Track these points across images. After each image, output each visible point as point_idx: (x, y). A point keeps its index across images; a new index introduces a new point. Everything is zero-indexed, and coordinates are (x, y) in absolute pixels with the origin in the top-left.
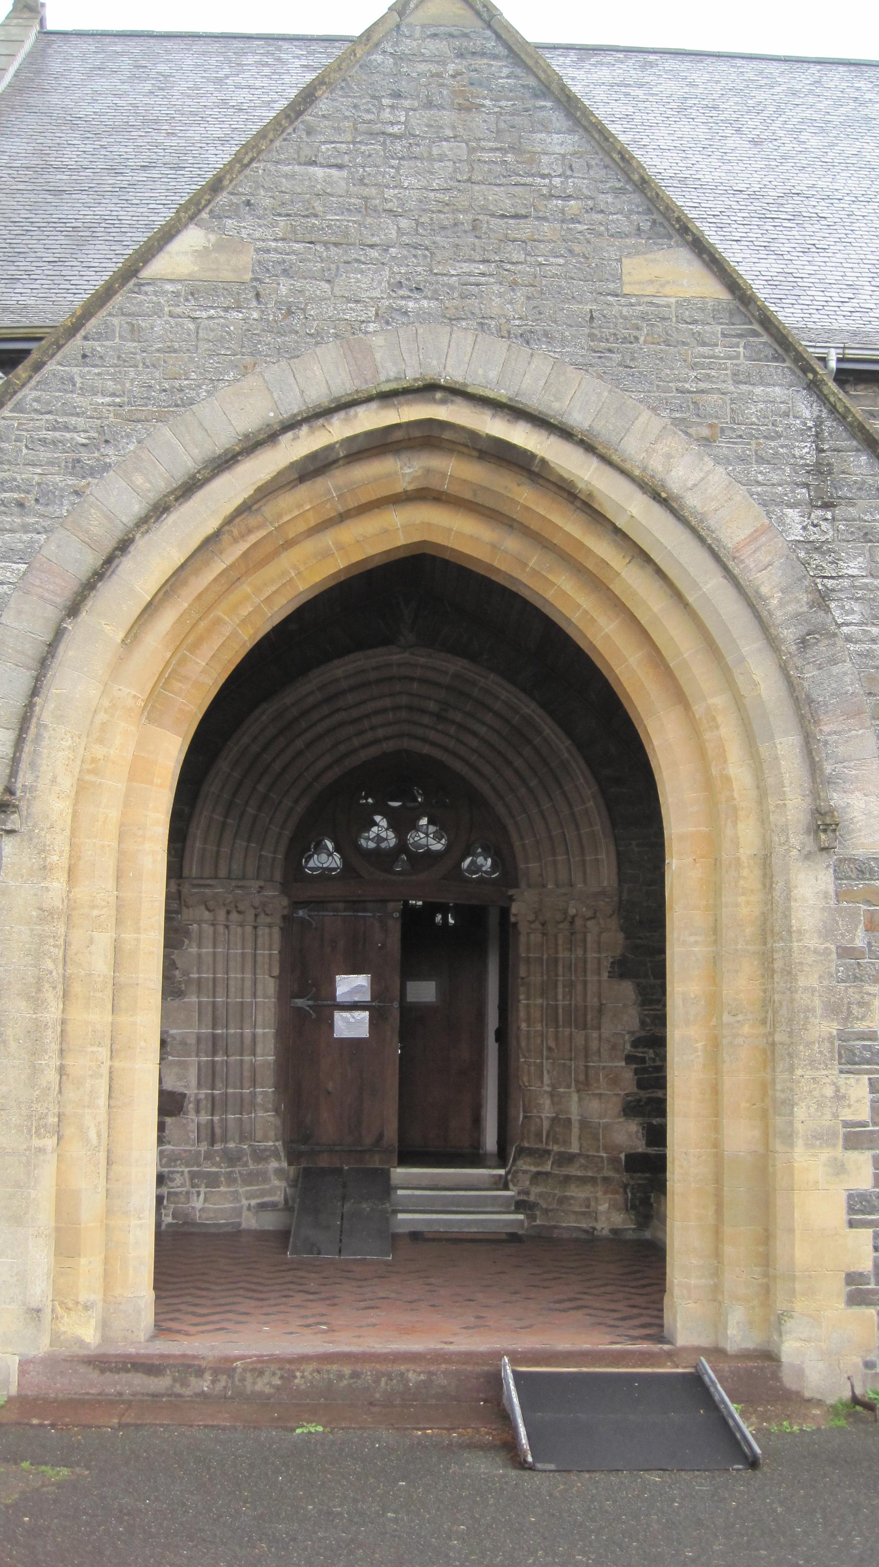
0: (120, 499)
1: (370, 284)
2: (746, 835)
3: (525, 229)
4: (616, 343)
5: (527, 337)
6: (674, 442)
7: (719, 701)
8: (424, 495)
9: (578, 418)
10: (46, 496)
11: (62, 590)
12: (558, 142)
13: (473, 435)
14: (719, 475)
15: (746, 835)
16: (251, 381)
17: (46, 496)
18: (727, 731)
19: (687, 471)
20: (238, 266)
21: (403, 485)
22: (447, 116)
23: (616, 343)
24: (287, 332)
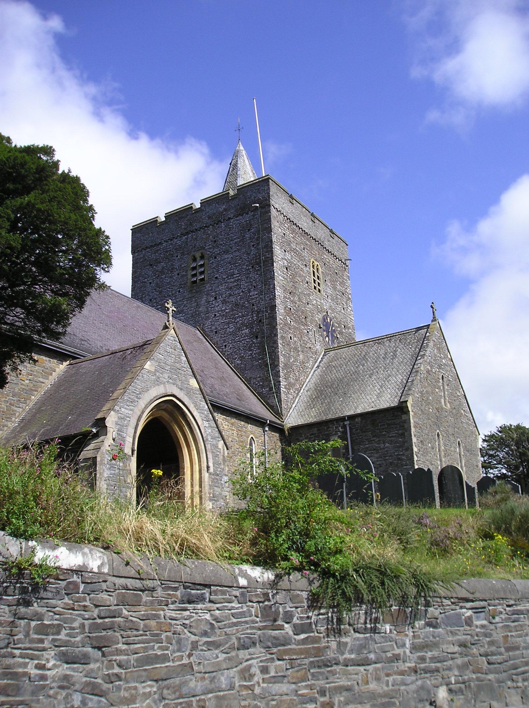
0: (142, 404)
1: (166, 376)
3: (180, 371)
4: (189, 391)
6: (194, 409)
8: (165, 410)
9: (186, 403)
11: (137, 417)
12: (184, 359)
14: (198, 415)
18: (195, 452)
19: (195, 413)
20: (153, 369)
21: (163, 408)
22: (173, 351)
23: (189, 391)
24: (158, 382)
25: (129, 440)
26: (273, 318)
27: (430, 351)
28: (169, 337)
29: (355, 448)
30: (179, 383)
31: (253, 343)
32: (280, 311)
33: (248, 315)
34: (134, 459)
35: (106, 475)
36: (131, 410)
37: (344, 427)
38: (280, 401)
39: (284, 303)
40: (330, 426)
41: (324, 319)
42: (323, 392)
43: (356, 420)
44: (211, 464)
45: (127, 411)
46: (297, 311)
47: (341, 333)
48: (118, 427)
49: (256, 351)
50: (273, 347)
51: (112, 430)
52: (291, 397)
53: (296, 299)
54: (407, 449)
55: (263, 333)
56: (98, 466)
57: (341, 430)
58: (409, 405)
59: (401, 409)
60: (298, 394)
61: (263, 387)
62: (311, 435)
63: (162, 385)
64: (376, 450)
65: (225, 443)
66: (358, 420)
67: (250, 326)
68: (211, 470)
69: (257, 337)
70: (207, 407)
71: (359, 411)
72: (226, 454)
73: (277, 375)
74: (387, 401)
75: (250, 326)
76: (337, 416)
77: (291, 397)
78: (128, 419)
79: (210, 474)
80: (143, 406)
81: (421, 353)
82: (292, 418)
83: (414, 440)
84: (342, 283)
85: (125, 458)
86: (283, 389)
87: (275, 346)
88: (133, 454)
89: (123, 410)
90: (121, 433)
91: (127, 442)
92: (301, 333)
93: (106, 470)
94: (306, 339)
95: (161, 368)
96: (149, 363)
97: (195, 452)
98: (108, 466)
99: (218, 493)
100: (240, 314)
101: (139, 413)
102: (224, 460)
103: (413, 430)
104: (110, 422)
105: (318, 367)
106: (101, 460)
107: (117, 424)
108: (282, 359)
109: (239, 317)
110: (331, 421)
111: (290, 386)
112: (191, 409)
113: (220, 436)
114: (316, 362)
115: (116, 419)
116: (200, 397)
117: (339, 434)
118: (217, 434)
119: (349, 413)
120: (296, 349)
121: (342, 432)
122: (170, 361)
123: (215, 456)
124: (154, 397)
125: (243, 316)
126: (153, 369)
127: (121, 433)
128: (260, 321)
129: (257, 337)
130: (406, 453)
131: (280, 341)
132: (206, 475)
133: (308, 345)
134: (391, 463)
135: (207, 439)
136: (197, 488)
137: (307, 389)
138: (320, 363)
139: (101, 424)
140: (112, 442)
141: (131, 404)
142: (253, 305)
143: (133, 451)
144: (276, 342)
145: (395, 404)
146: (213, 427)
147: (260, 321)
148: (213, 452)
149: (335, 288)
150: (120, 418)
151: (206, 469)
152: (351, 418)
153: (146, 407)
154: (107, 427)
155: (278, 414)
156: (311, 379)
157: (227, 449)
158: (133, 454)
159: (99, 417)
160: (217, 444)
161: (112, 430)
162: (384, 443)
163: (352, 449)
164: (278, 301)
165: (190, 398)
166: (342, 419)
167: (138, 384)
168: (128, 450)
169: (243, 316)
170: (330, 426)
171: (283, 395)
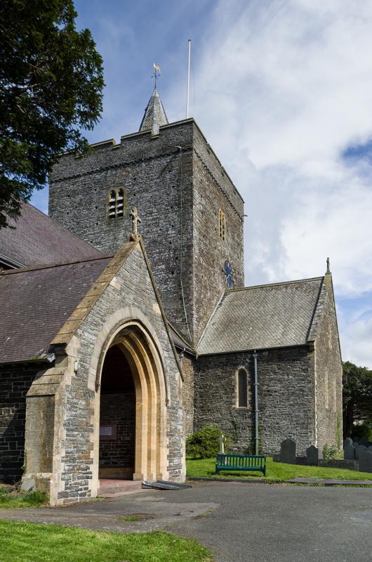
0: (107, 328)
1: (131, 297)
2: (155, 401)
4: (152, 318)
5: (145, 314)
7: (154, 379)
10: (99, 324)
11: (101, 344)
12: (149, 280)
13: (140, 329)
15: (155, 401)
16: (119, 311)
17: (99, 324)
18: (154, 384)
20: (118, 287)
22: (139, 269)
24: (123, 304)
25: (93, 372)
26: (190, 257)
27: (325, 299)
28: (135, 252)
29: (261, 377)
30: (143, 307)
31: (169, 278)
32: (196, 250)
33: (165, 252)
34: (98, 395)
35: (65, 418)
36: (95, 335)
37: (252, 359)
38: (192, 331)
39: (199, 244)
40: (239, 357)
41: (226, 264)
42: (228, 325)
43: (264, 353)
44: (169, 398)
45: (90, 336)
46: (208, 253)
47: (236, 278)
48: (80, 356)
49: (171, 285)
50: (188, 283)
51: (73, 360)
52: (200, 328)
53: (207, 242)
54: (310, 382)
55: (179, 270)
56: (56, 407)
57: (248, 361)
58: (315, 344)
59: (307, 348)
60: (205, 326)
61: (176, 318)
62: (221, 363)
63: (127, 308)
64: (280, 381)
65: (181, 375)
66: (266, 354)
67: (166, 262)
68: (169, 405)
69: (173, 273)
70: (167, 336)
71: (267, 345)
72: (181, 386)
73: (190, 309)
74: (294, 338)
75: (166, 262)
76: (245, 349)
77: (200, 328)
78: (91, 346)
79: (168, 408)
80: (109, 331)
81: (320, 300)
82: (202, 349)
83: (316, 375)
84: (239, 236)
85: (88, 395)
86: (195, 321)
87: (190, 282)
88: (96, 390)
89: (86, 334)
90: (84, 364)
91: (90, 375)
92: (210, 274)
93: (65, 411)
94: (212, 279)
95: (126, 287)
96: (114, 279)
97: (154, 384)
98: (68, 406)
99: (174, 428)
100: (157, 250)
101: (103, 339)
102: (180, 393)
103: (316, 366)
104: (71, 350)
105: (220, 304)
106: (61, 399)
107: (79, 352)
108: (195, 294)
109: (156, 253)
110: (240, 353)
111: (200, 319)
112: (153, 336)
113: (177, 368)
114: (218, 300)
115: (78, 346)
116: (161, 324)
117: (247, 364)
118: (175, 366)
119: (257, 348)
120: (205, 287)
121: (250, 363)
122: (135, 280)
123: (173, 389)
124: (120, 321)
125: (160, 252)
126: (118, 287)
127: (84, 364)
128: (177, 258)
129: (173, 273)
130: (309, 385)
131: (194, 279)
132: (164, 409)
133: (214, 285)
134: (293, 393)
135: (167, 371)
136: (154, 424)
137: (212, 322)
138: (222, 301)
139: (60, 351)
140: (74, 375)
141: (95, 328)
142: (171, 243)
143: (97, 386)
144: (190, 279)
145: (302, 341)
146: (171, 358)
147: (177, 258)
148: (171, 385)
149: (234, 239)
150: (83, 345)
151: (165, 403)
152: (259, 351)
153: (111, 333)
154: (67, 355)
155: (191, 343)
156: (216, 315)
157: (183, 381)
158: (96, 390)
159: (57, 340)
160: (175, 376)
161: (73, 360)
162: (288, 375)
163: (258, 378)
164: (195, 242)
165: (153, 325)
166: (251, 352)
167: (104, 304)
168: (91, 386)
169: (160, 252)
170: (239, 357)
171: (194, 327)
